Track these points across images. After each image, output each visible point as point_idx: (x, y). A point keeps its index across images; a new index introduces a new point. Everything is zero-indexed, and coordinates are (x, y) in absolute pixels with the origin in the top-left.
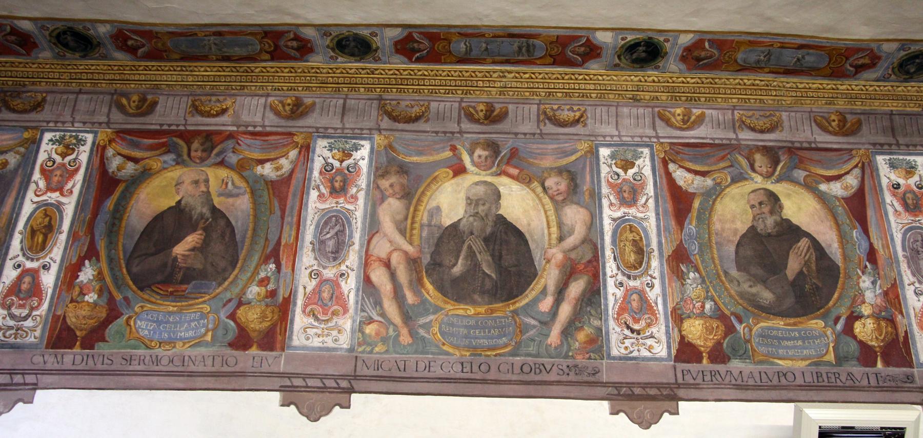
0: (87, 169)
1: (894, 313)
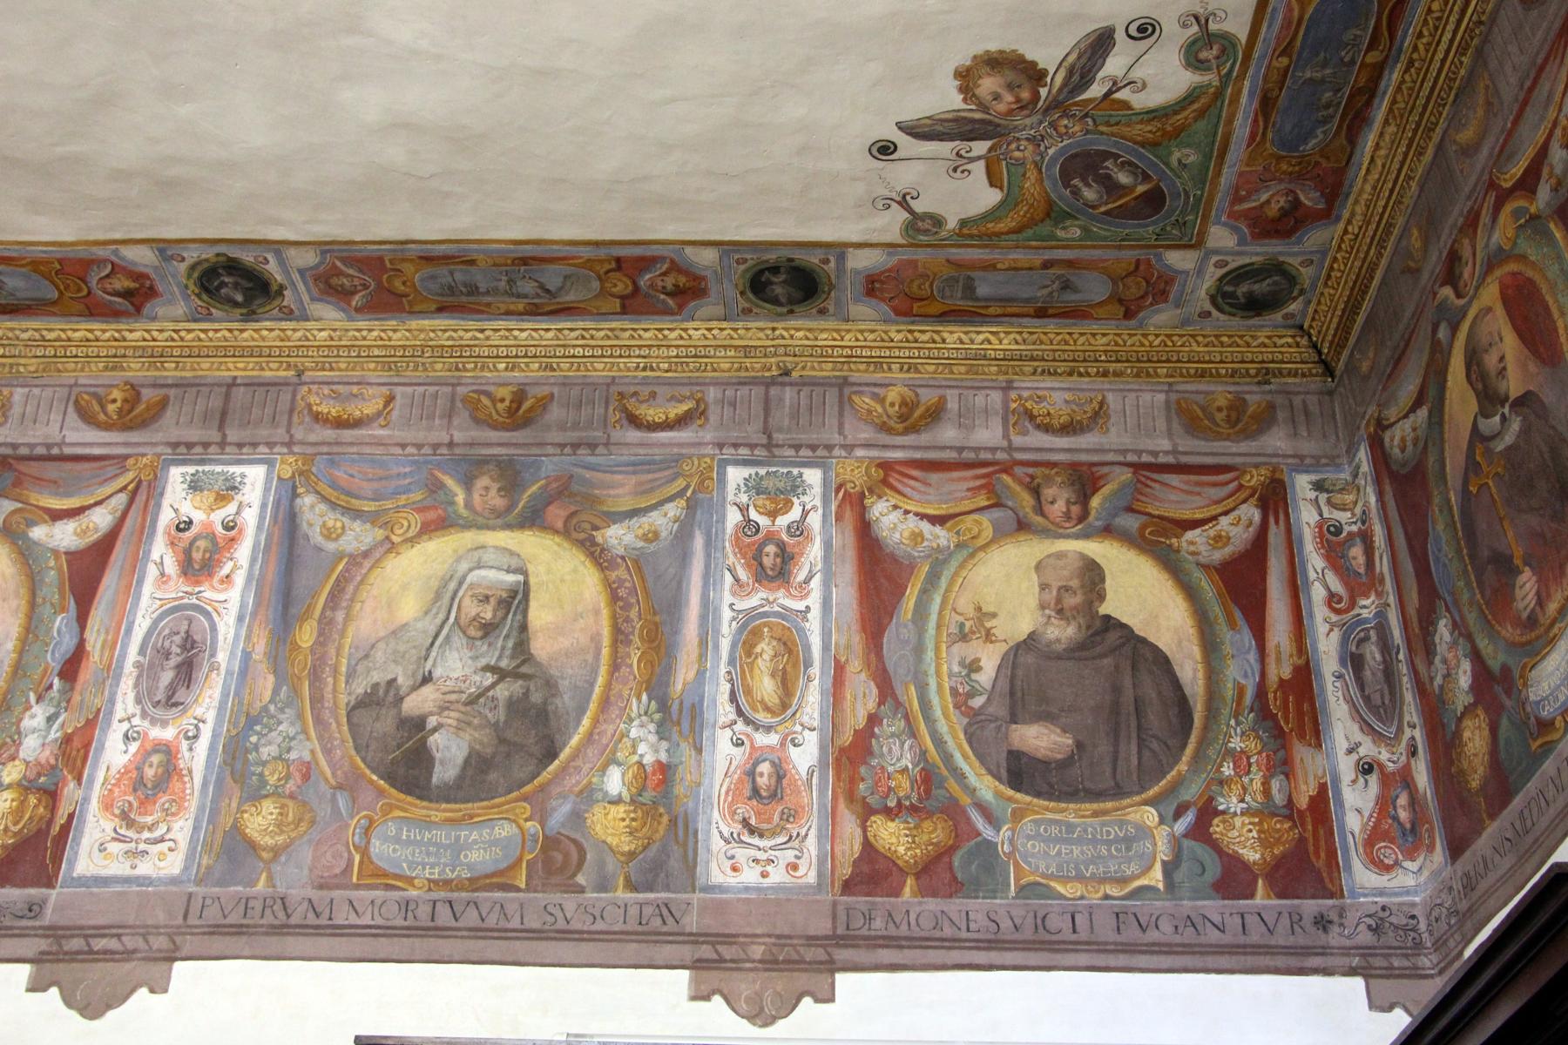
1: (65, 778)
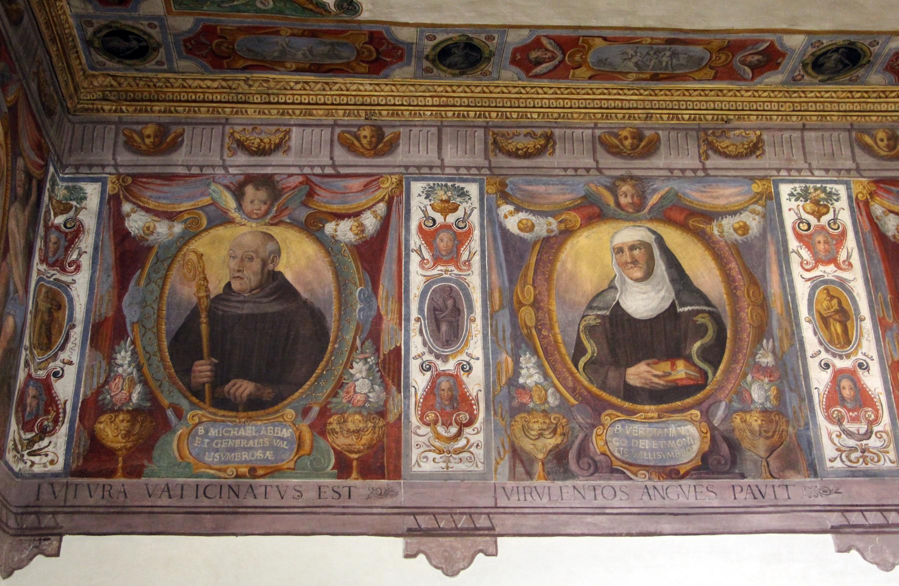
0: (856, 233)
